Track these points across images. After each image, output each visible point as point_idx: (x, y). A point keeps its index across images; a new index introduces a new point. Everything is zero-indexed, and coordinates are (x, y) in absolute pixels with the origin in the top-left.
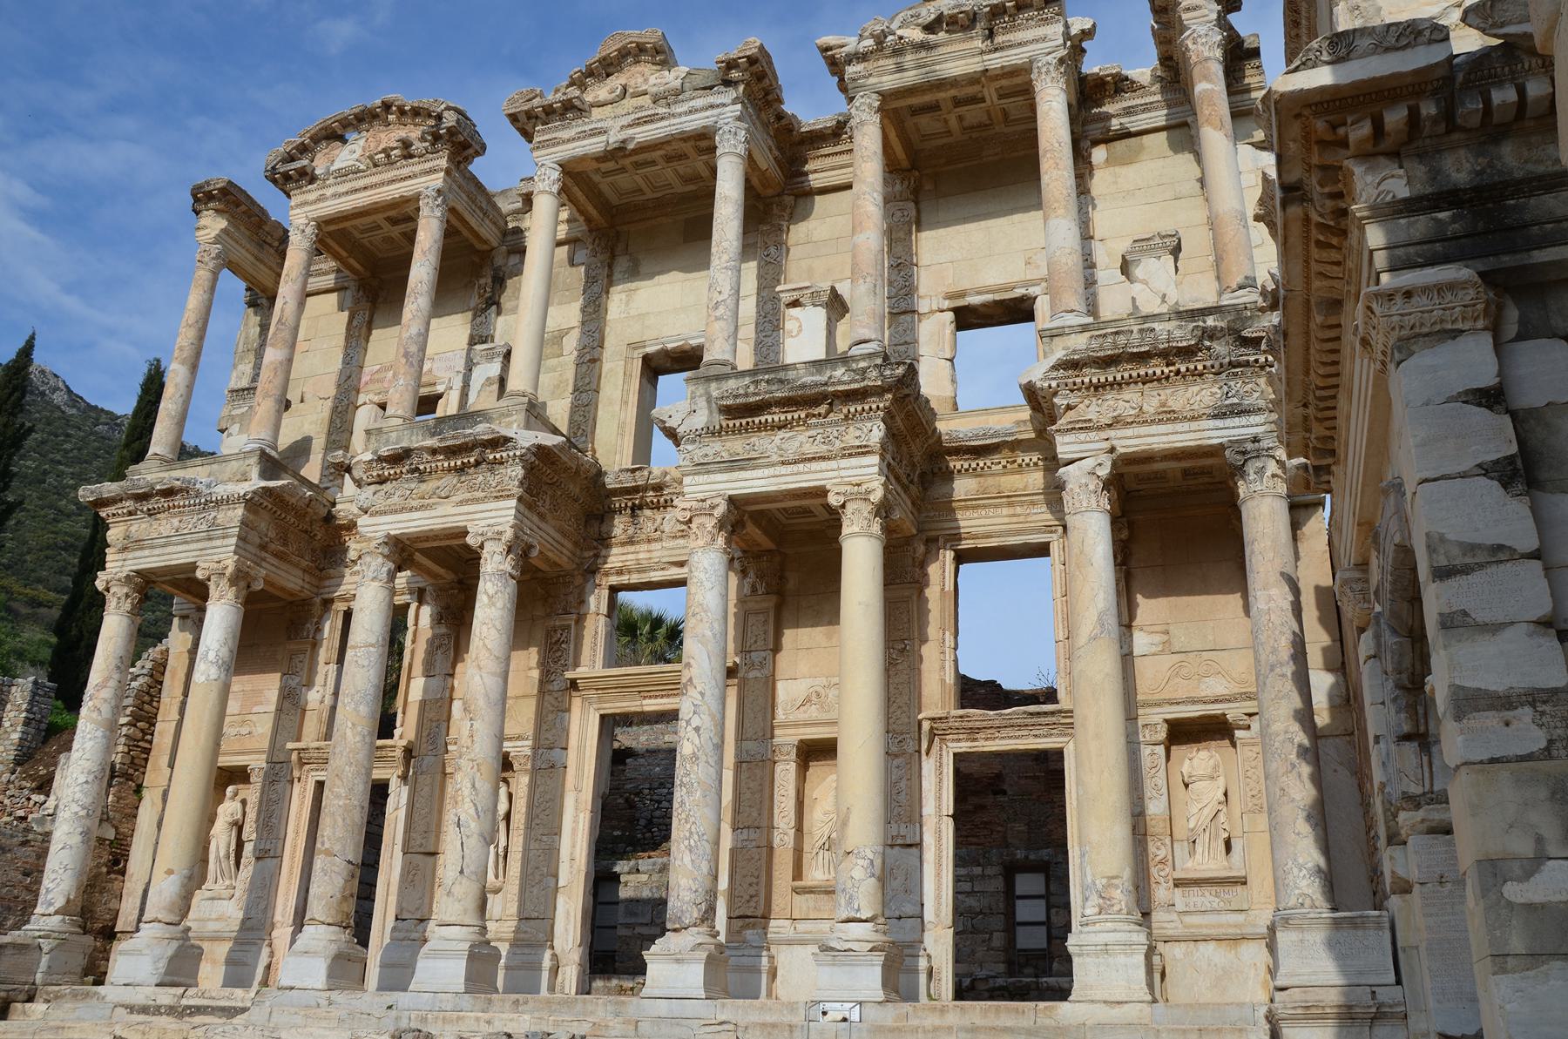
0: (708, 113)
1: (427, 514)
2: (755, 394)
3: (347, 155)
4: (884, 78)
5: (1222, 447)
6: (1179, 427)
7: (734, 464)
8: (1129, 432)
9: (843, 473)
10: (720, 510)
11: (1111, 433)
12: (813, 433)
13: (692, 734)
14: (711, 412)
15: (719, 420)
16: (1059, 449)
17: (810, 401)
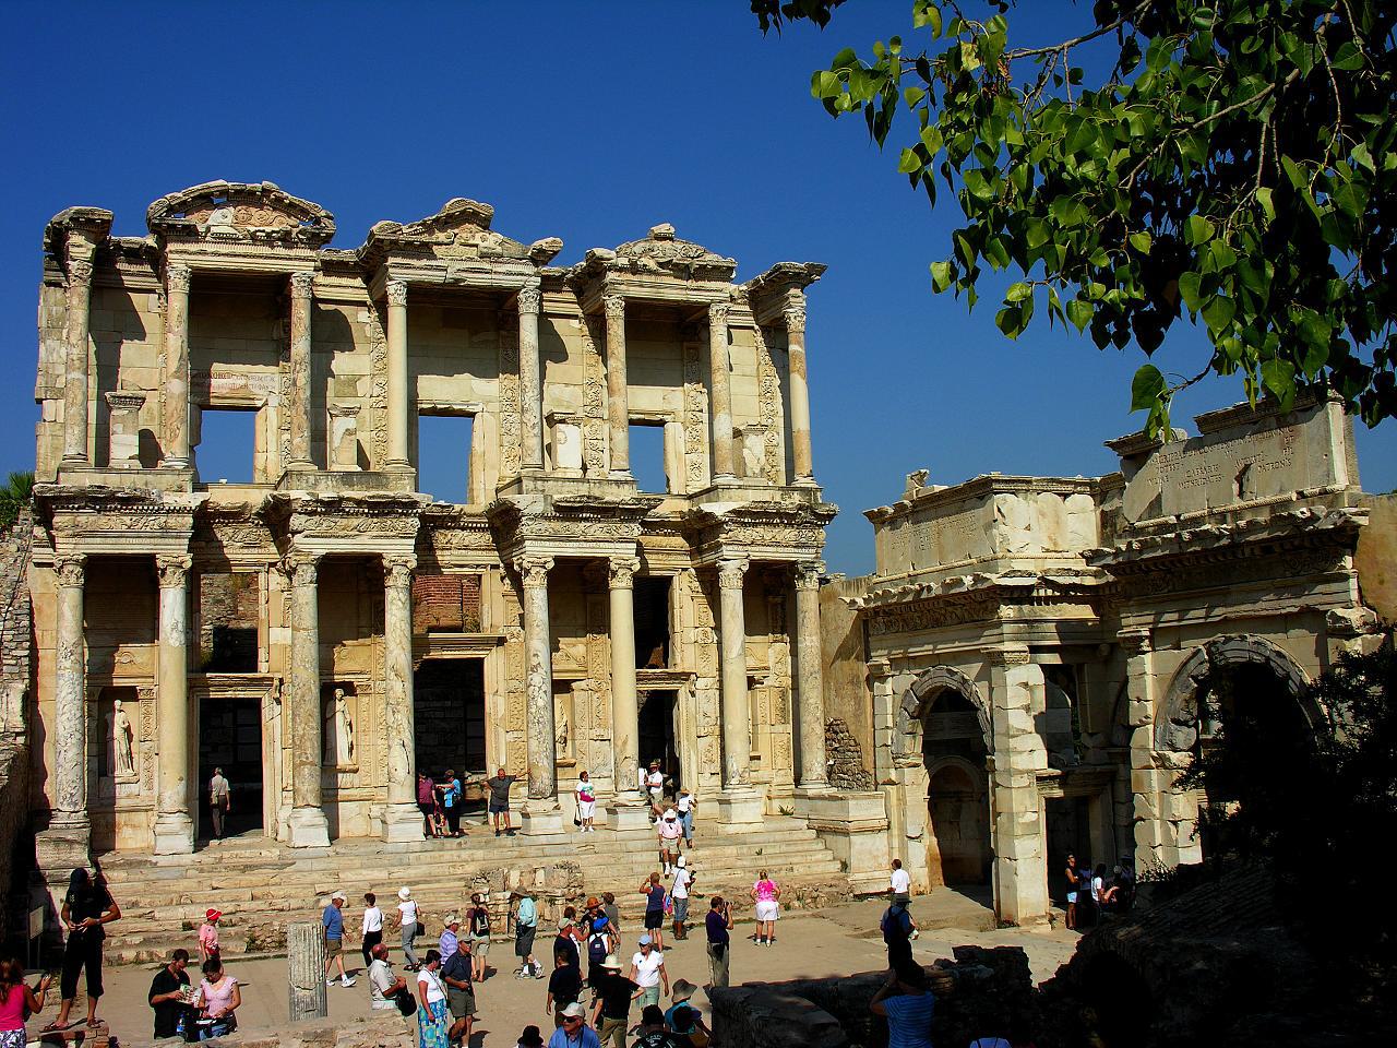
0: (519, 277)
1: (349, 541)
2: (580, 502)
3: (220, 220)
4: (631, 288)
5: (795, 563)
6: (779, 549)
7: (555, 538)
8: (757, 549)
9: (617, 551)
10: (551, 565)
11: (749, 548)
12: (599, 525)
13: (543, 695)
14: (546, 505)
15: (551, 511)
16: (725, 553)
17: (607, 512)
